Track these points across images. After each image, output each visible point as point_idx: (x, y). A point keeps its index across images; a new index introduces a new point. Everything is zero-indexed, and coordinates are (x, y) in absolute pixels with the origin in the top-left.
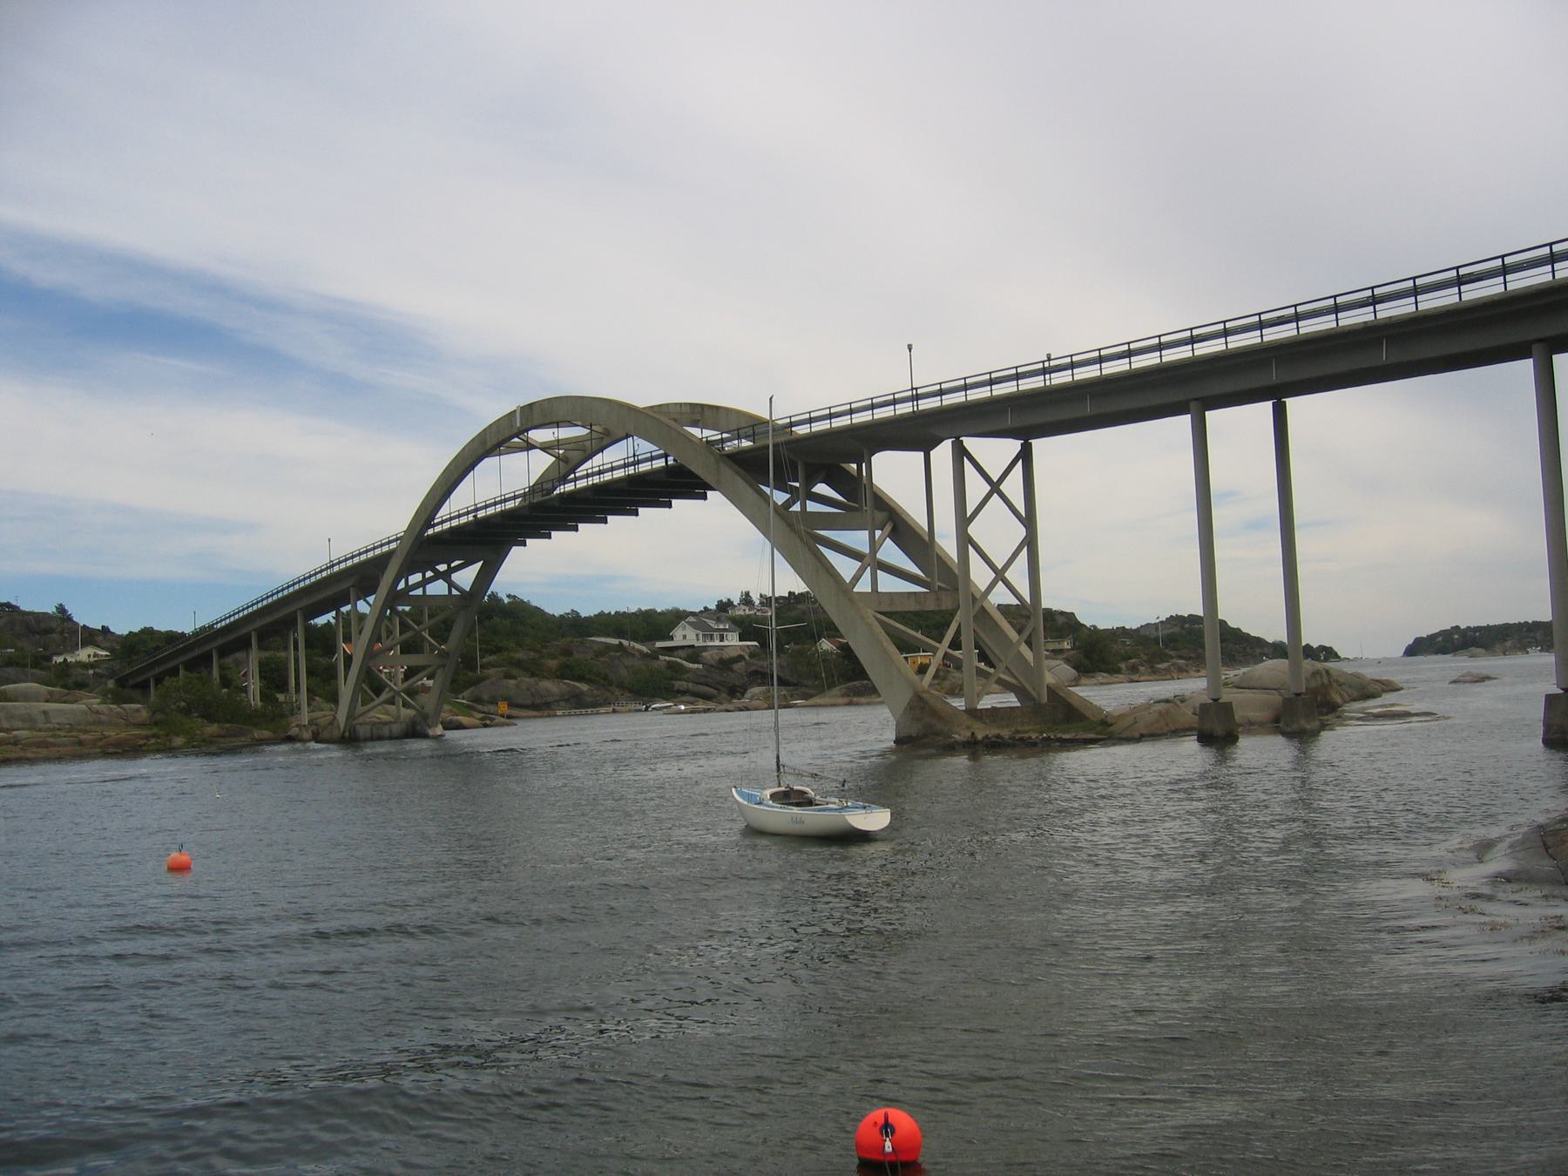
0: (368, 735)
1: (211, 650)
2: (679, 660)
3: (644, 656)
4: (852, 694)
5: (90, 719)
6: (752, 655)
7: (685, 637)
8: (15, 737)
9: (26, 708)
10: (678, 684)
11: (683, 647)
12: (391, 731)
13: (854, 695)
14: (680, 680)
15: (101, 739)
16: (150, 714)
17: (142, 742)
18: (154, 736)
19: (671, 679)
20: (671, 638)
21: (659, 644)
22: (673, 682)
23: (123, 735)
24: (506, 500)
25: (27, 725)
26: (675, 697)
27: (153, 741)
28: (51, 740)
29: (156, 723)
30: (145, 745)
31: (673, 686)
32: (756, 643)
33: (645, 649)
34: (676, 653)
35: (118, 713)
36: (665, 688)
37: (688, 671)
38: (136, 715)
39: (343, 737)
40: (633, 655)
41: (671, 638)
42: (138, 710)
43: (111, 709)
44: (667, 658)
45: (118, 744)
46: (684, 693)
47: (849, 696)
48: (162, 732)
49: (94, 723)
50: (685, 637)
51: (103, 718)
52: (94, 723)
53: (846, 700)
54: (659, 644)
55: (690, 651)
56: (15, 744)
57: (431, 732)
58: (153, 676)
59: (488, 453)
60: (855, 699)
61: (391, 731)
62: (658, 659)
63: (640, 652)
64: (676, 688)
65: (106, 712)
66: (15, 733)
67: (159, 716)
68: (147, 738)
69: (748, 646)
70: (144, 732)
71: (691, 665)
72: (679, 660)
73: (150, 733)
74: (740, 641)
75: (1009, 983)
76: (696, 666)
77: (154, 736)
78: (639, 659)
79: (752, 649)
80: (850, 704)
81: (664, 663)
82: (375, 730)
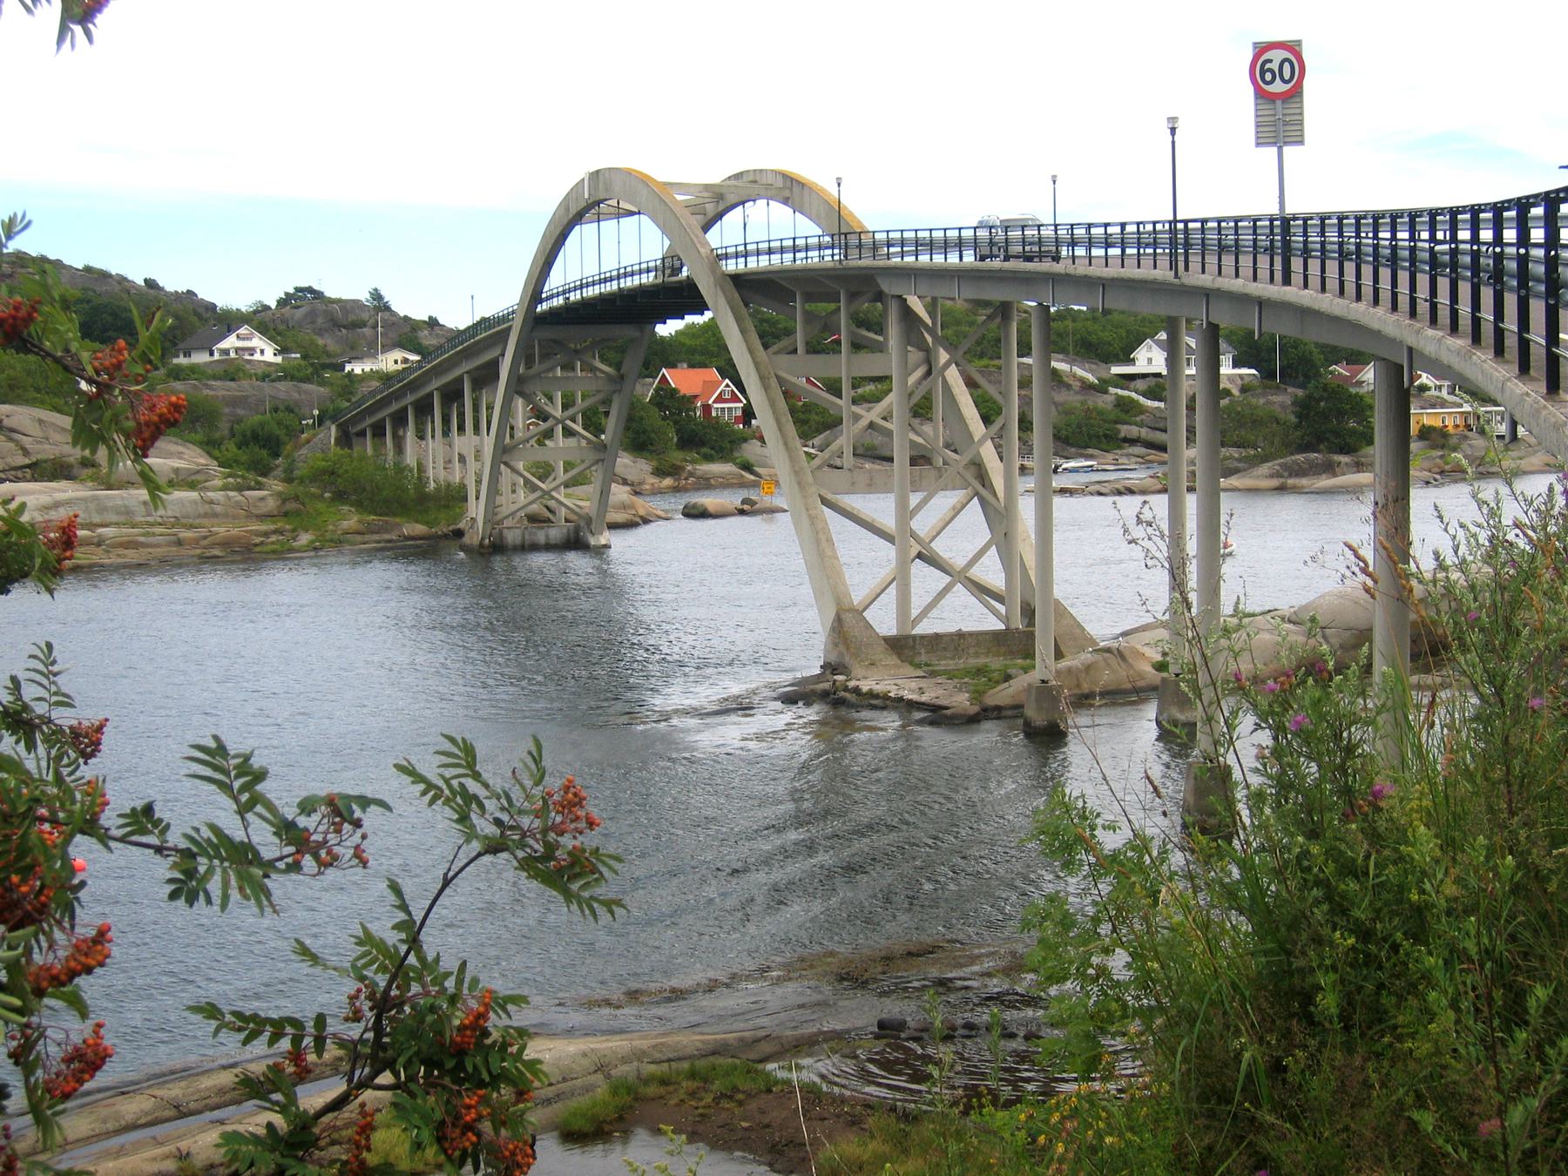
0: (518, 541)
1: (430, 395)
2: (1134, 395)
3: (1087, 387)
4: (1286, 474)
5: (201, 511)
6: (1244, 389)
7: (1150, 360)
8: (100, 536)
9: (123, 498)
10: (1126, 430)
11: (1144, 376)
12: (547, 537)
13: (1290, 476)
14: (1130, 424)
15: (205, 538)
16: (279, 502)
17: (258, 540)
18: (275, 532)
19: (1116, 422)
20: (1132, 362)
21: (1116, 370)
22: (1119, 426)
23: (235, 532)
24: (605, 280)
25: (122, 519)
26: (1120, 448)
27: (273, 538)
28: (142, 539)
29: (286, 514)
30: (262, 543)
31: (1119, 431)
32: (1253, 371)
33: (1091, 378)
34: (1132, 385)
35: (237, 502)
36: (1106, 436)
37: (1142, 410)
38: (260, 504)
39: (481, 545)
40: (1069, 387)
41: (1132, 362)
42: (262, 499)
43: (229, 498)
44: (1120, 392)
45: (226, 544)
46: (1132, 442)
47: (1281, 476)
48: (288, 527)
49: (206, 515)
50: (1150, 360)
51: (218, 509)
52: (206, 515)
53: (1275, 482)
54: (1116, 370)
55: (1153, 381)
56: (99, 545)
57: (592, 541)
58: (389, 415)
59: (578, 219)
60: (1291, 482)
61: (547, 537)
62: (1106, 392)
63: (1082, 380)
64: (1122, 435)
65: (222, 500)
66: (100, 530)
67: (291, 506)
68: (266, 534)
69: (1241, 376)
70: (264, 527)
71: (1149, 403)
72: (1134, 395)
73: (272, 527)
74: (1234, 367)
75: (962, 944)
76: (1156, 404)
77: (275, 532)
78: (1076, 393)
79: (1247, 380)
80: (1281, 489)
81: (1113, 397)
82: (527, 537)
